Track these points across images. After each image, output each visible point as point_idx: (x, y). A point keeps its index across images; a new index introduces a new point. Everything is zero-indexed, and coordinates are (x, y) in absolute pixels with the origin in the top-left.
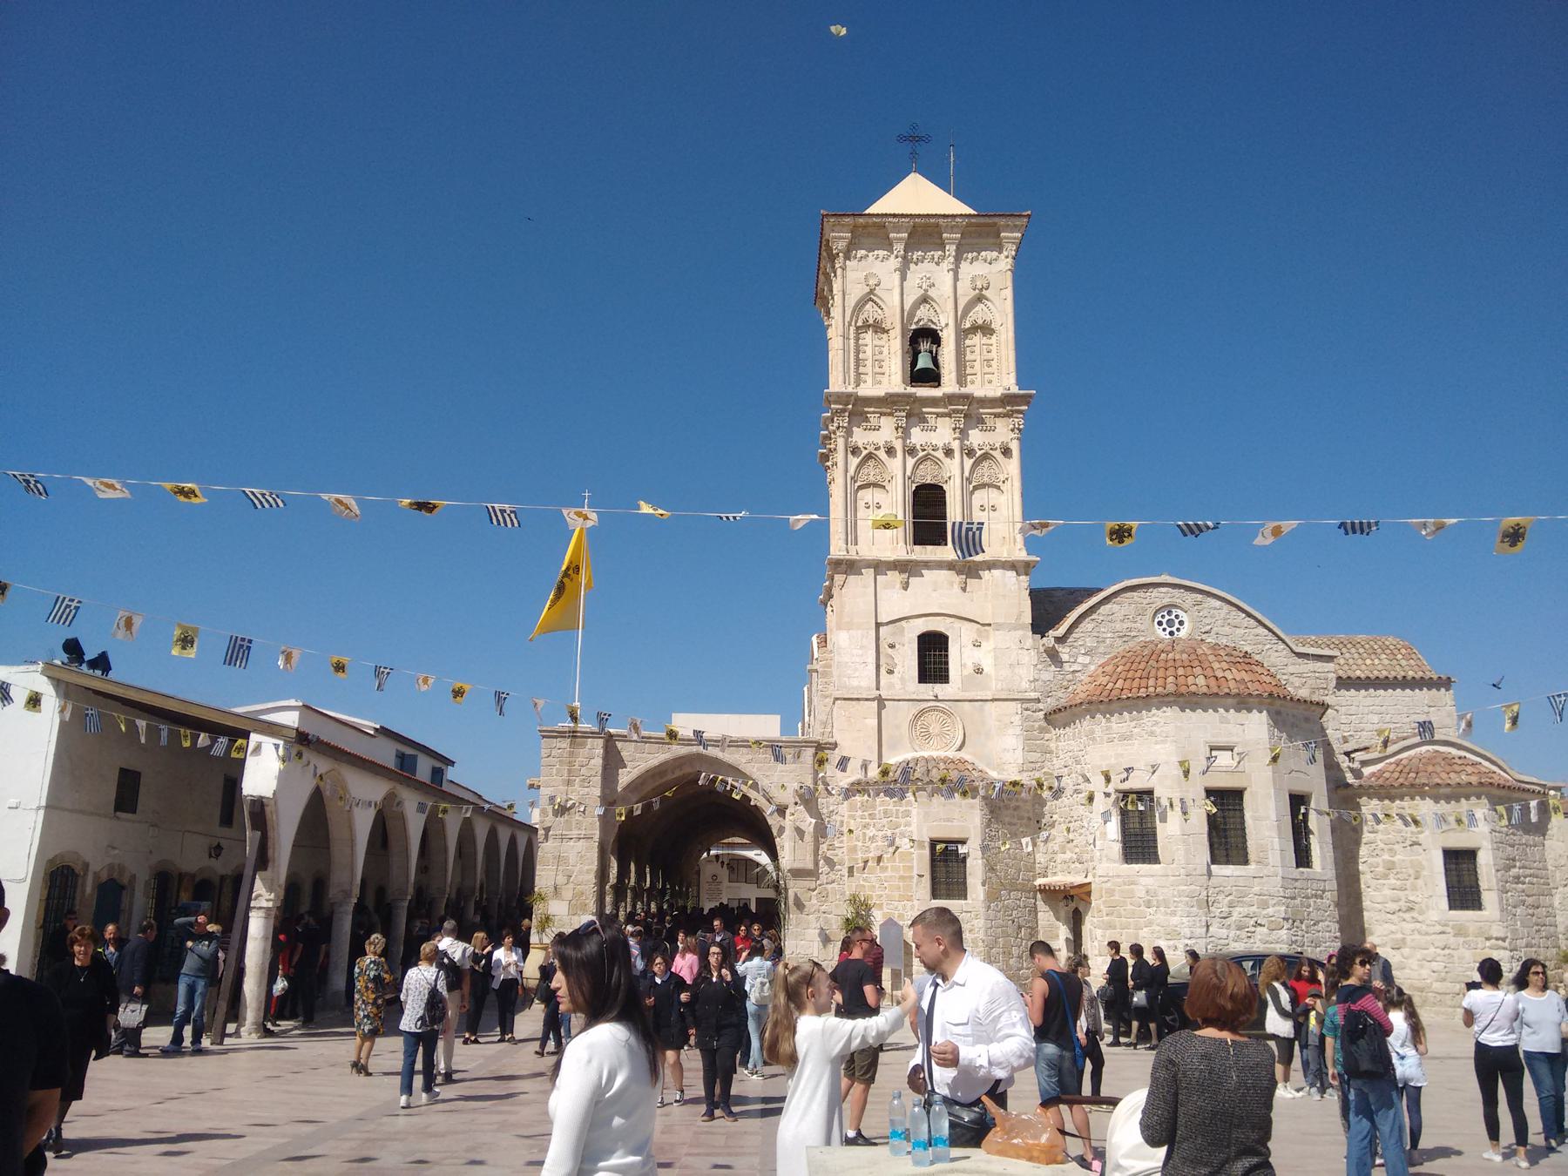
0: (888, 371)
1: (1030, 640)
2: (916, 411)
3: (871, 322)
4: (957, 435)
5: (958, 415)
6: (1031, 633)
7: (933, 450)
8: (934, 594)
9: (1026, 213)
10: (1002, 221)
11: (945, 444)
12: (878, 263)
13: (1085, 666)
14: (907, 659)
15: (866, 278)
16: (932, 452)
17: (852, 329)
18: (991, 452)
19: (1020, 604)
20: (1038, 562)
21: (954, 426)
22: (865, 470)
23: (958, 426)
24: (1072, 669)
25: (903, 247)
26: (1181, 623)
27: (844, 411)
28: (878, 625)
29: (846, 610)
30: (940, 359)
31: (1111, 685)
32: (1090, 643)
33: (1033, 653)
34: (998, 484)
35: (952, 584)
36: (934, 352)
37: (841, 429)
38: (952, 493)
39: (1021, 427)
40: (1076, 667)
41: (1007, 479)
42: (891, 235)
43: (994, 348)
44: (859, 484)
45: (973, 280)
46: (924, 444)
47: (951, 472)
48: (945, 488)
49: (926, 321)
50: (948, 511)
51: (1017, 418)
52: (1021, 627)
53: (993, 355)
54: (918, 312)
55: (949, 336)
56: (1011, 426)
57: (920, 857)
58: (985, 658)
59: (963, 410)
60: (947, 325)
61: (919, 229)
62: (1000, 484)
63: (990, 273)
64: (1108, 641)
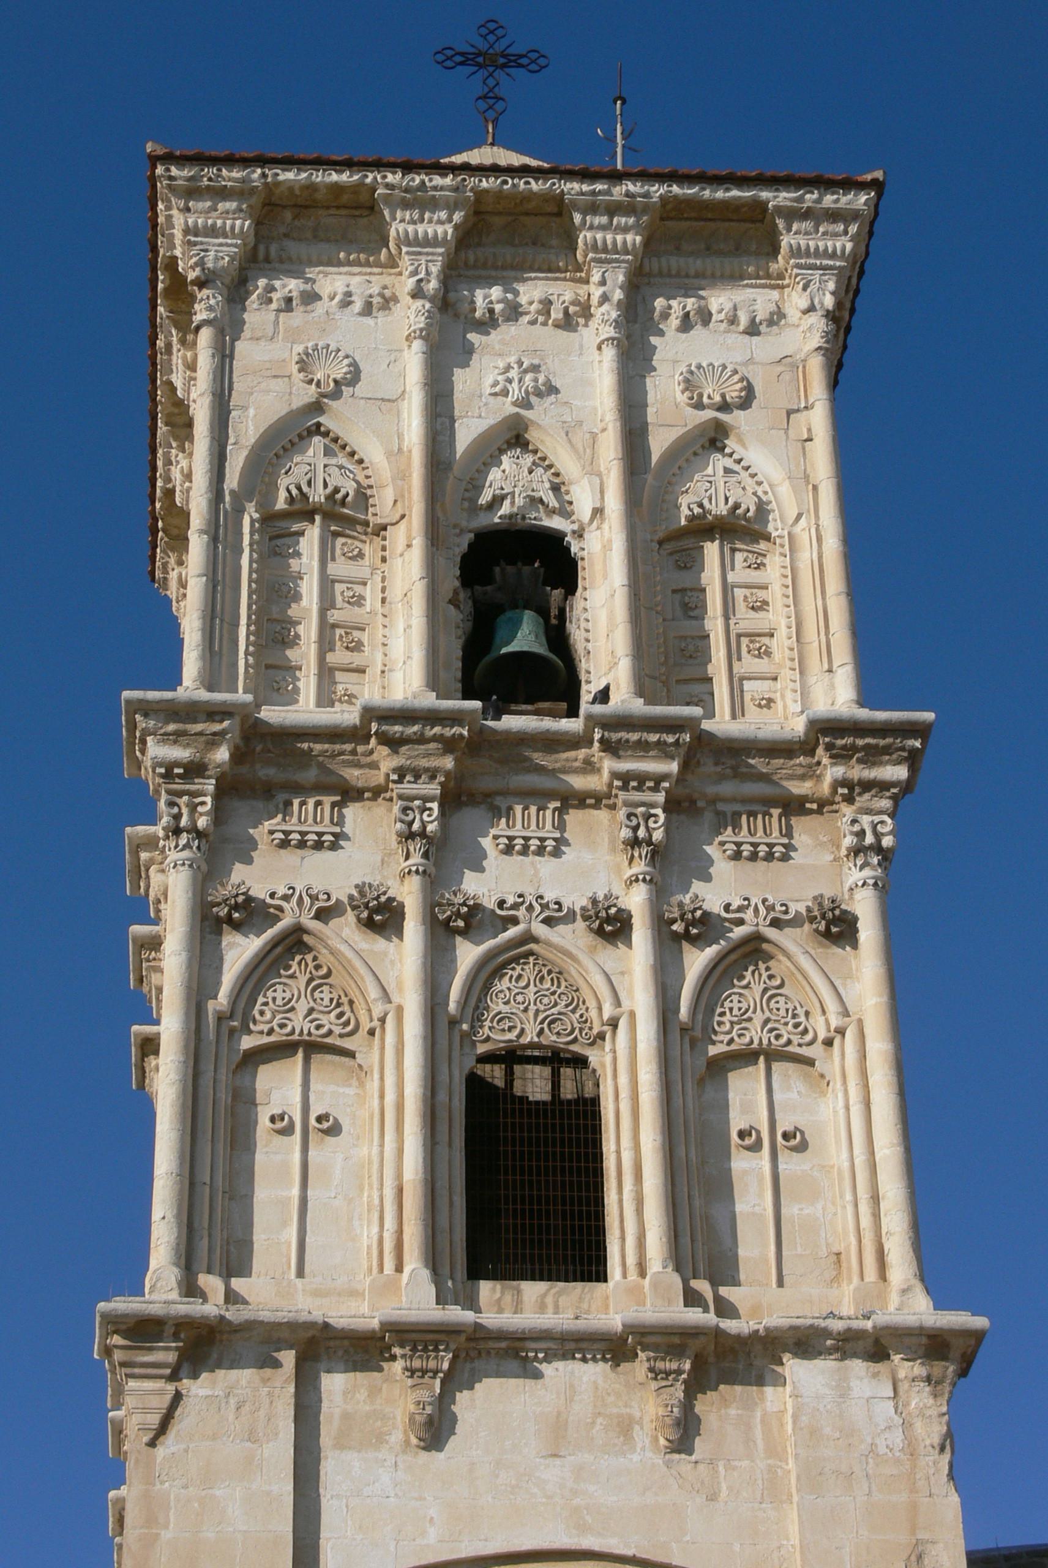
0: (379, 657)
2: (486, 783)
3: (318, 495)
4: (640, 867)
5: (637, 796)
7: (548, 922)
8: (553, 1473)
9: (869, 177)
10: (779, 198)
11: (594, 901)
12: (349, 319)
15: (304, 365)
16: (540, 930)
17: (250, 515)
18: (771, 933)
19: (914, 1507)
20: (979, 1336)
21: (625, 833)
22: (277, 993)
23: (642, 833)
25: (435, 269)
27: (195, 770)
29: (166, 1535)
30: (577, 635)
34: (805, 1051)
35: (625, 1427)
36: (554, 612)
37: (184, 839)
38: (623, 1080)
39: (887, 842)
41: (841, 1031)
42: (400, 225)
43: (776, 594)
44: (247, 1042)
45: (689, 384)
46: (511, 900)
47: (618, 1003)
49: (519, 501)
50: (609, 1147)
51: (869, 812)
53: (778, 617)
54: (494, 475)
55: (607, 547)
56: (849, 841)
59: (664, 777)
60: (598, 512)
61: (498, 221)
62: (815, 1051)
63: (751, 361)
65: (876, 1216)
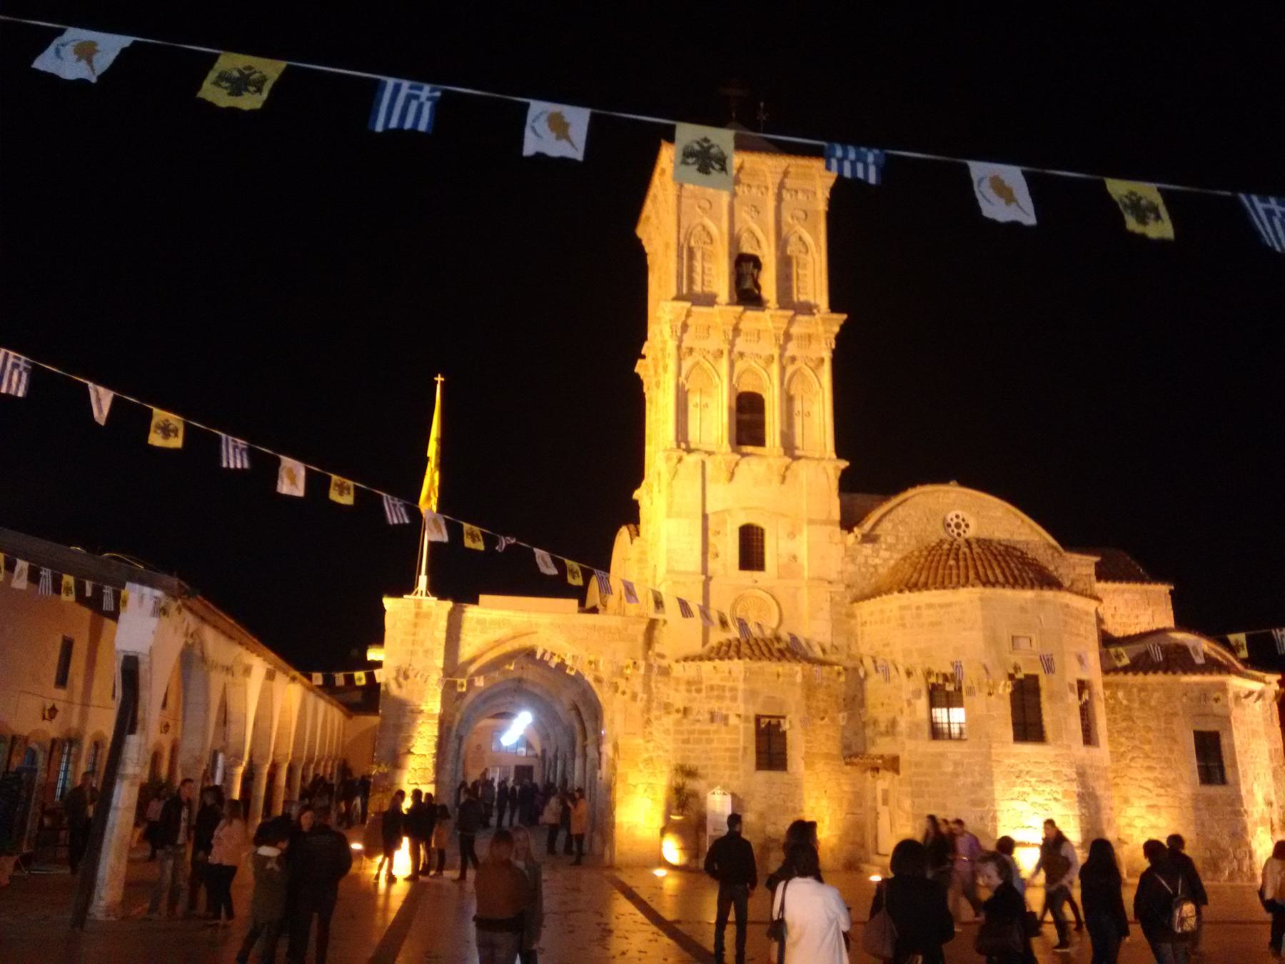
1: (839, 537)
6: (838, 529)
13: (885, 560)
14: (729, 547)
24: (873, 563)
26: (967, 526)
28: (705, 517)
31: (916, 575)
32: (890, 540)
33: (841, 547)
40: (877, 561)
48: (764, 396)
52: (827, 522)
57: (746, 729)
58: (801, 546)
64: (906, 540)
65: (825, 435)
